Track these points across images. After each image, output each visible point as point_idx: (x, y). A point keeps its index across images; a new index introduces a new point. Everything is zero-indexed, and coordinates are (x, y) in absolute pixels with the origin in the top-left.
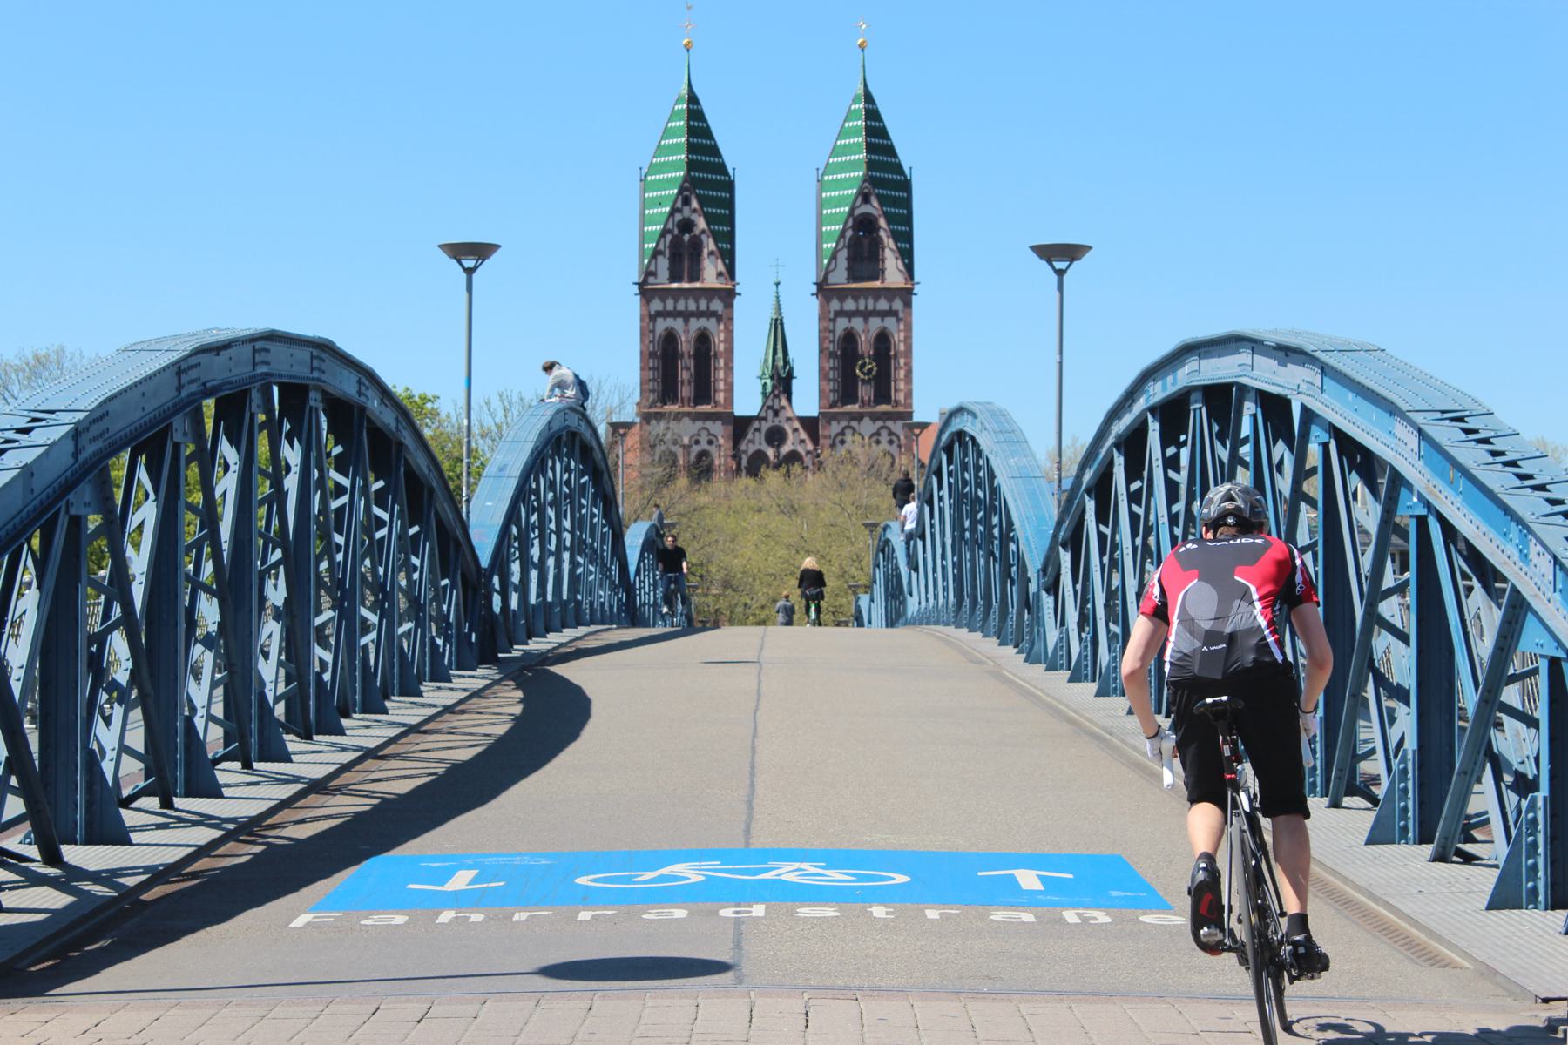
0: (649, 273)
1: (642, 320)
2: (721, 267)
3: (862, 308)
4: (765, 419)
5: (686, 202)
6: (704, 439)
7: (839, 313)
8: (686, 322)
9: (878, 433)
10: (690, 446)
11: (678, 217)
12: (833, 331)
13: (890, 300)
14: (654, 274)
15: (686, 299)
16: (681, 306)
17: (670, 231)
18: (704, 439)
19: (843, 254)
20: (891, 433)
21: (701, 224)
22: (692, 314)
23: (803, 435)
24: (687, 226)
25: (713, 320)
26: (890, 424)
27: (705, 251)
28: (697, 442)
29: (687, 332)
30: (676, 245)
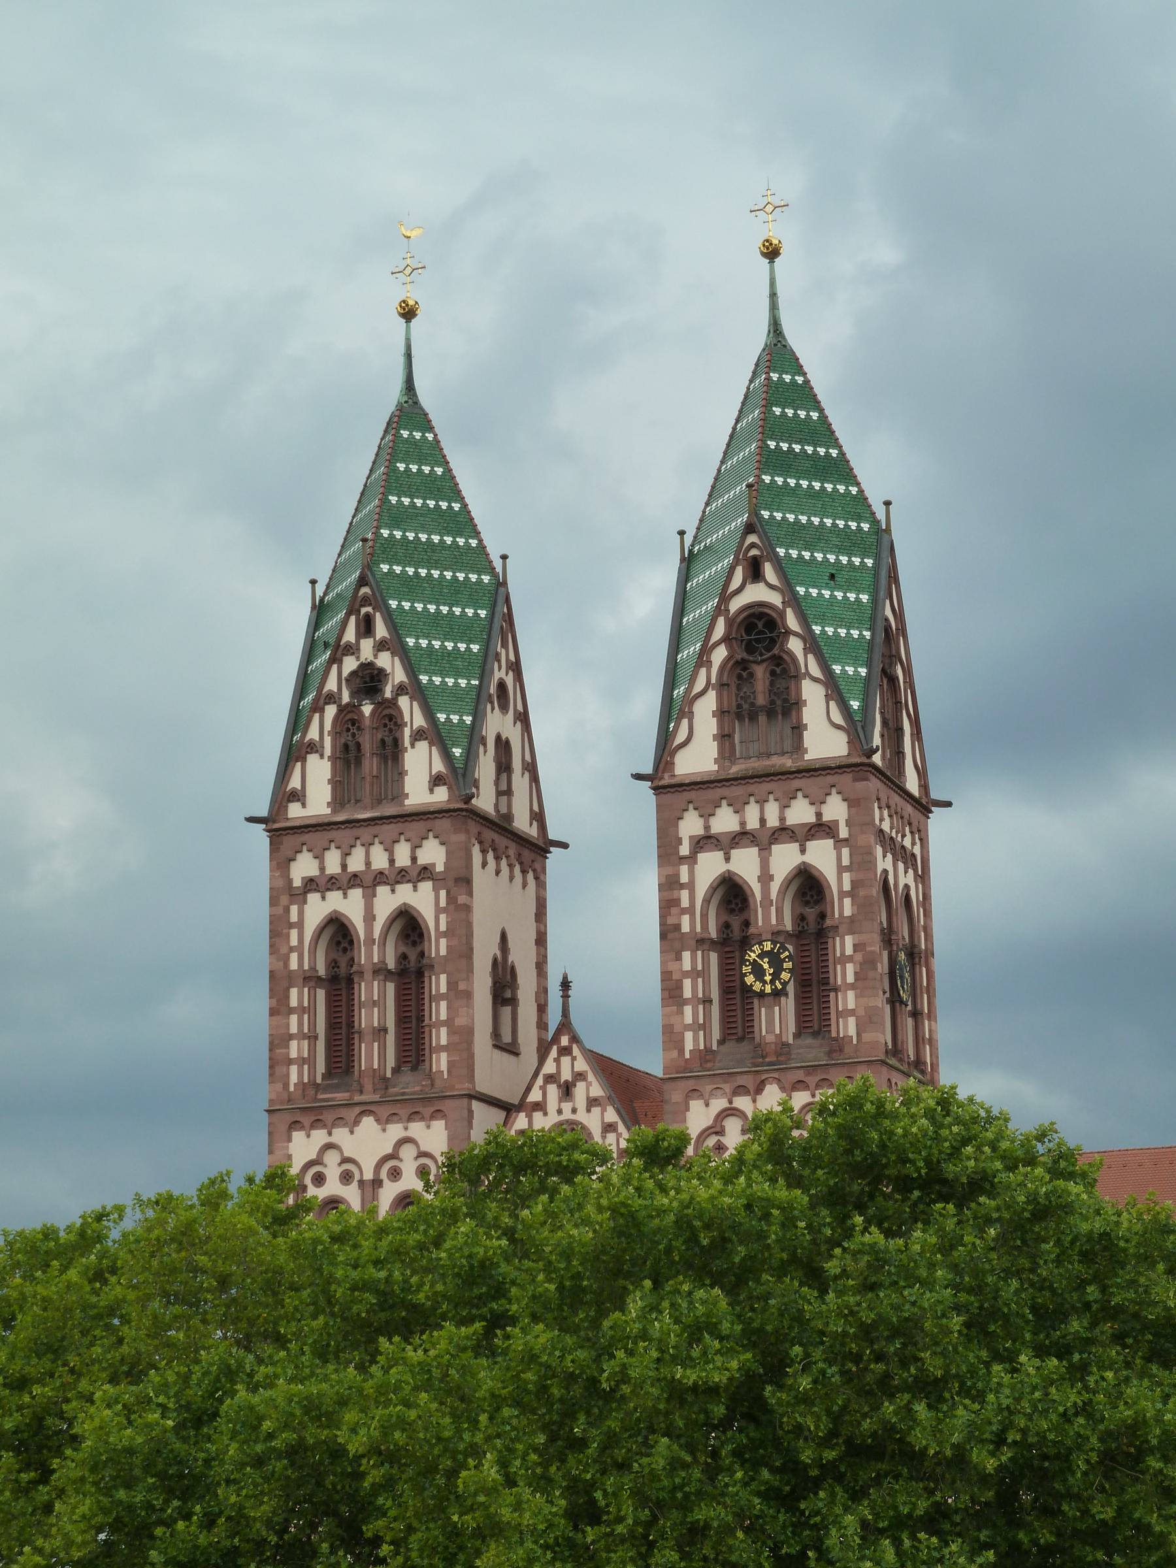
0: (284, 795)
1: (274, 901)
2: (439, 766)
3: (753, 823)
4: (540, 1106)
5: (366, 628)
6: (409, 1164)
7: (706, 841)
8: (370, 897)
10: (377, 1183)
11: (350, 664)
12: (691, 885)
13: (817, 802)
14: (298, 796)
15: (368, 845)
16: (356, 863)
17: (331, 698)
18: (409, 1164)
19: (706, 708)
21: (398, 675)
22: (380, 878)
24: (369, 681)
25: (426, 887)
27: (407, 732)
28: (395, 1174)
29: (369, 917)
30: (348, 720)
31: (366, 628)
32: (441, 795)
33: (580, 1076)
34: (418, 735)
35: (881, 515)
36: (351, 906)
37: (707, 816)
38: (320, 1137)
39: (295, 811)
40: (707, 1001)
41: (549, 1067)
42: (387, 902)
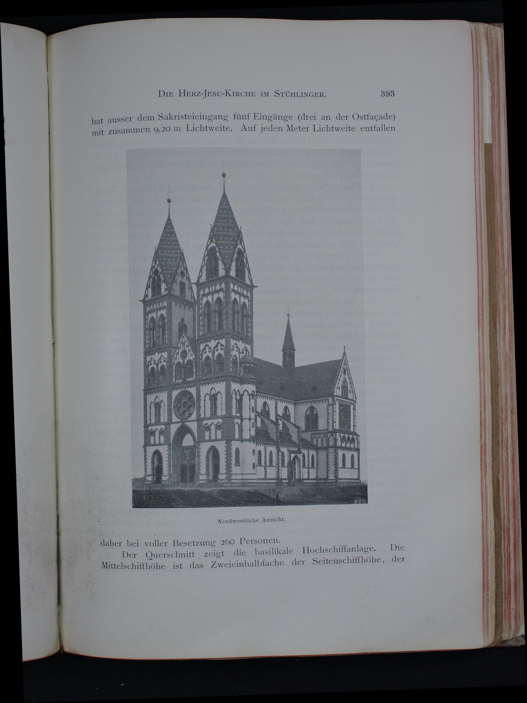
0: (146, 296)
2: (166, 287)
4: (180, 348)
5: (156, 263)
9: (216, 346)
18: (162, 361)
20: (222, 345)
21: (160, 271)
23: (192, 353)
25: (165, 310)
26: (220, 341)
29: (157, 316)
31: (156, 263)
32: (166, 292)
33: (185, 341)
34: (163, 282)
35: (240, 228)
36: (154, 315)
37: (204, 290)
38: (150, 357)
39: (147, 299)
40: (204, 325)
41: (181, 340)
42: (159, 314)
